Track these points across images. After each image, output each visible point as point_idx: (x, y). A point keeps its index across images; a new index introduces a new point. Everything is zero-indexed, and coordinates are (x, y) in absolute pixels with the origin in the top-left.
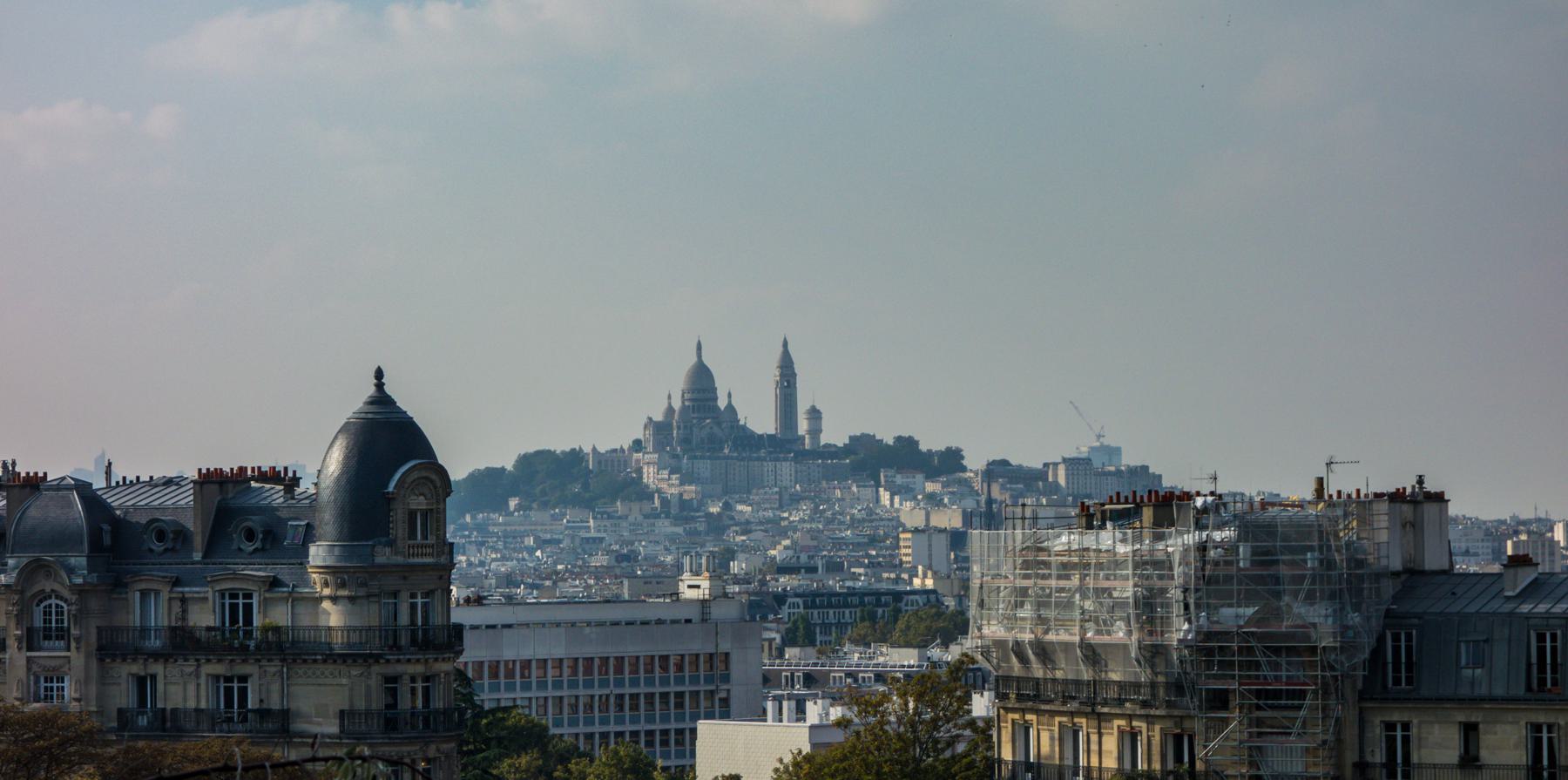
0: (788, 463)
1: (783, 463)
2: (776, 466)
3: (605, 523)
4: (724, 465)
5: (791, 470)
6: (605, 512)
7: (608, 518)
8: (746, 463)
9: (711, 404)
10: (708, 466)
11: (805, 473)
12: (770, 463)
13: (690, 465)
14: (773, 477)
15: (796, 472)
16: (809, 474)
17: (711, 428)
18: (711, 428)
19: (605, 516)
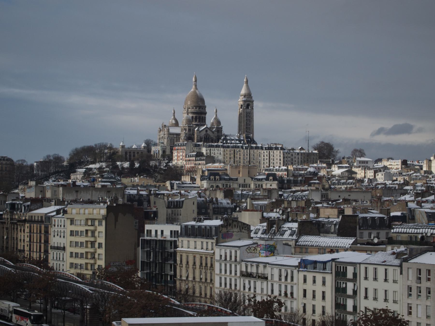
0: (278, 151)
1: (275, 151)
2: (269, 153)
3: (217, 184)
4: (233, 152)
5: (280, 156)
6: (218, 174)
7: (221, 179)
8: (248, 151)
9: (204, 116)
10: (222, 153)
11: (289, 159)
12: (265, 151)
13: (209, 151)
14: (268, 161)
15: (284, 158)
16: (292, 160)
17: (206, 131)
18: (206, 131)
19: (217, 177)
